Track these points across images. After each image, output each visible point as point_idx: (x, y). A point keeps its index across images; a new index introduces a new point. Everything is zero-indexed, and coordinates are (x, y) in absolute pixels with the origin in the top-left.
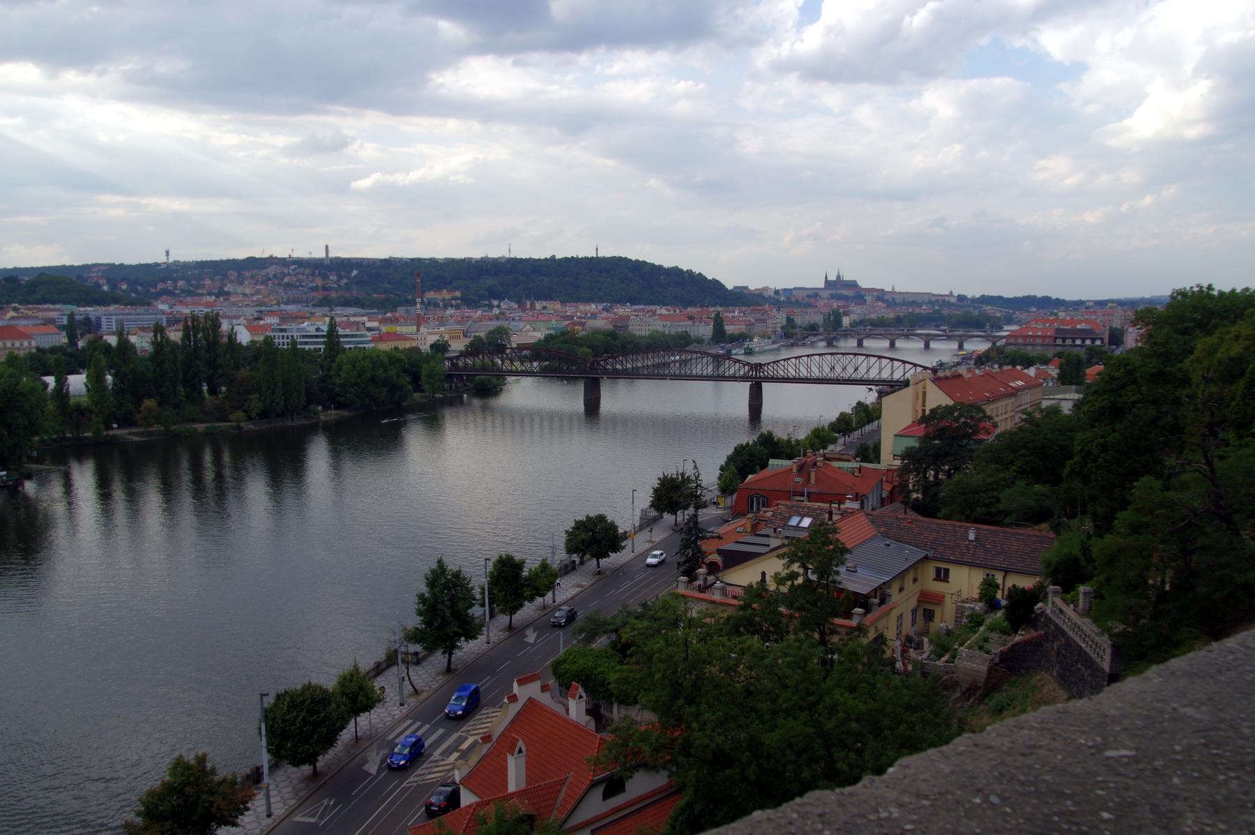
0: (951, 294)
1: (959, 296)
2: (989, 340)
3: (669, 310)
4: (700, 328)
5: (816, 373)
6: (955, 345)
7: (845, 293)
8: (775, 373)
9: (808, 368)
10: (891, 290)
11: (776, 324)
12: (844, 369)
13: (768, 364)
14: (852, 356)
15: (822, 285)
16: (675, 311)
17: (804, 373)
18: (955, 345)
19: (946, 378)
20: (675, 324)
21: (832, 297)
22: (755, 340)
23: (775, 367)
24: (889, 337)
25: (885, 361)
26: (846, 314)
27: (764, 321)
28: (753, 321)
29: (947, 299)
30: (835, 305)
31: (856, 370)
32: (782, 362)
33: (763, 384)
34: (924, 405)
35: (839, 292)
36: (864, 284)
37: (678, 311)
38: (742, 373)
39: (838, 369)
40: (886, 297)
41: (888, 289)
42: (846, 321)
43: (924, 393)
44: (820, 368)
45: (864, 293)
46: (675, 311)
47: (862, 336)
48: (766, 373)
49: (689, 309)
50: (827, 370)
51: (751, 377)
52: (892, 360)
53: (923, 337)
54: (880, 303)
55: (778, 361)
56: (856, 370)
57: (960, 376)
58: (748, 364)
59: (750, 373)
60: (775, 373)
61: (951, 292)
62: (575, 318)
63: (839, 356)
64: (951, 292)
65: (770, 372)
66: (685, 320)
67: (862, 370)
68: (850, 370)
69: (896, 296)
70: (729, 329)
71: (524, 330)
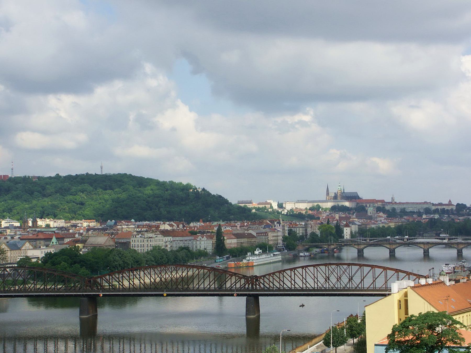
0: (450, 204)
1: (458, 205)
2: (454, 248)
3: (171, 225)
4: (202, 242)
5: (311, 284)
6: (453, 252)
7: (347, 204)
8: (271, 285)
9: (304, 279)
10: (390, 200)
11: (278, 236)
12: (339, 279)
13: (264, 276)
14: (345, 267)
15: (324, 197)
16: (178, 227)
17: (299, 284)
18: (453, 252)
19: (427, 285)
20: (177, 238)
21: (334, 209)
22: (257, 252)
23: (271, 280)
24: (388, 246)
25: (378, 271)
26: (347, 226)
27: (266, 234)
28: (254, 234)
29: (446, 208)
30: (337, 216)
31: (351, 279)
32: (277, 274)
33: (260, 298)
34: (407, 313)
35: (341, 204)
36: (365, 195)
37: (181, 226)
38: (238, 285)
39: (333, 279)
40: (388, 207)
41: (388, 200)
42: (347, 232)
43: (406, 301)
44: (315, 278)
45: (364, 205)
46: (178, 227)
47: (362, 247)
48: (262, 286)
49: (192, 225)
50: (322, 280)
51: (248, 290)
52: (385, 269)
53: (422, 246)
54: (381, 214)
55: (274, 273)
56: (351, 279)
57: (443, 282)
58: (244, 277)
59: (247, 286)
60: (271, 285)
61: (450, 201)
62: (77, 236)
63: (333, 267)
64: (450, 201)
65: (265, 284)
66: (187, 236)
67: (357, 279)
68: (345, 279)
69: (396, 206)
70: (231, 243)
71: (23, 248)
